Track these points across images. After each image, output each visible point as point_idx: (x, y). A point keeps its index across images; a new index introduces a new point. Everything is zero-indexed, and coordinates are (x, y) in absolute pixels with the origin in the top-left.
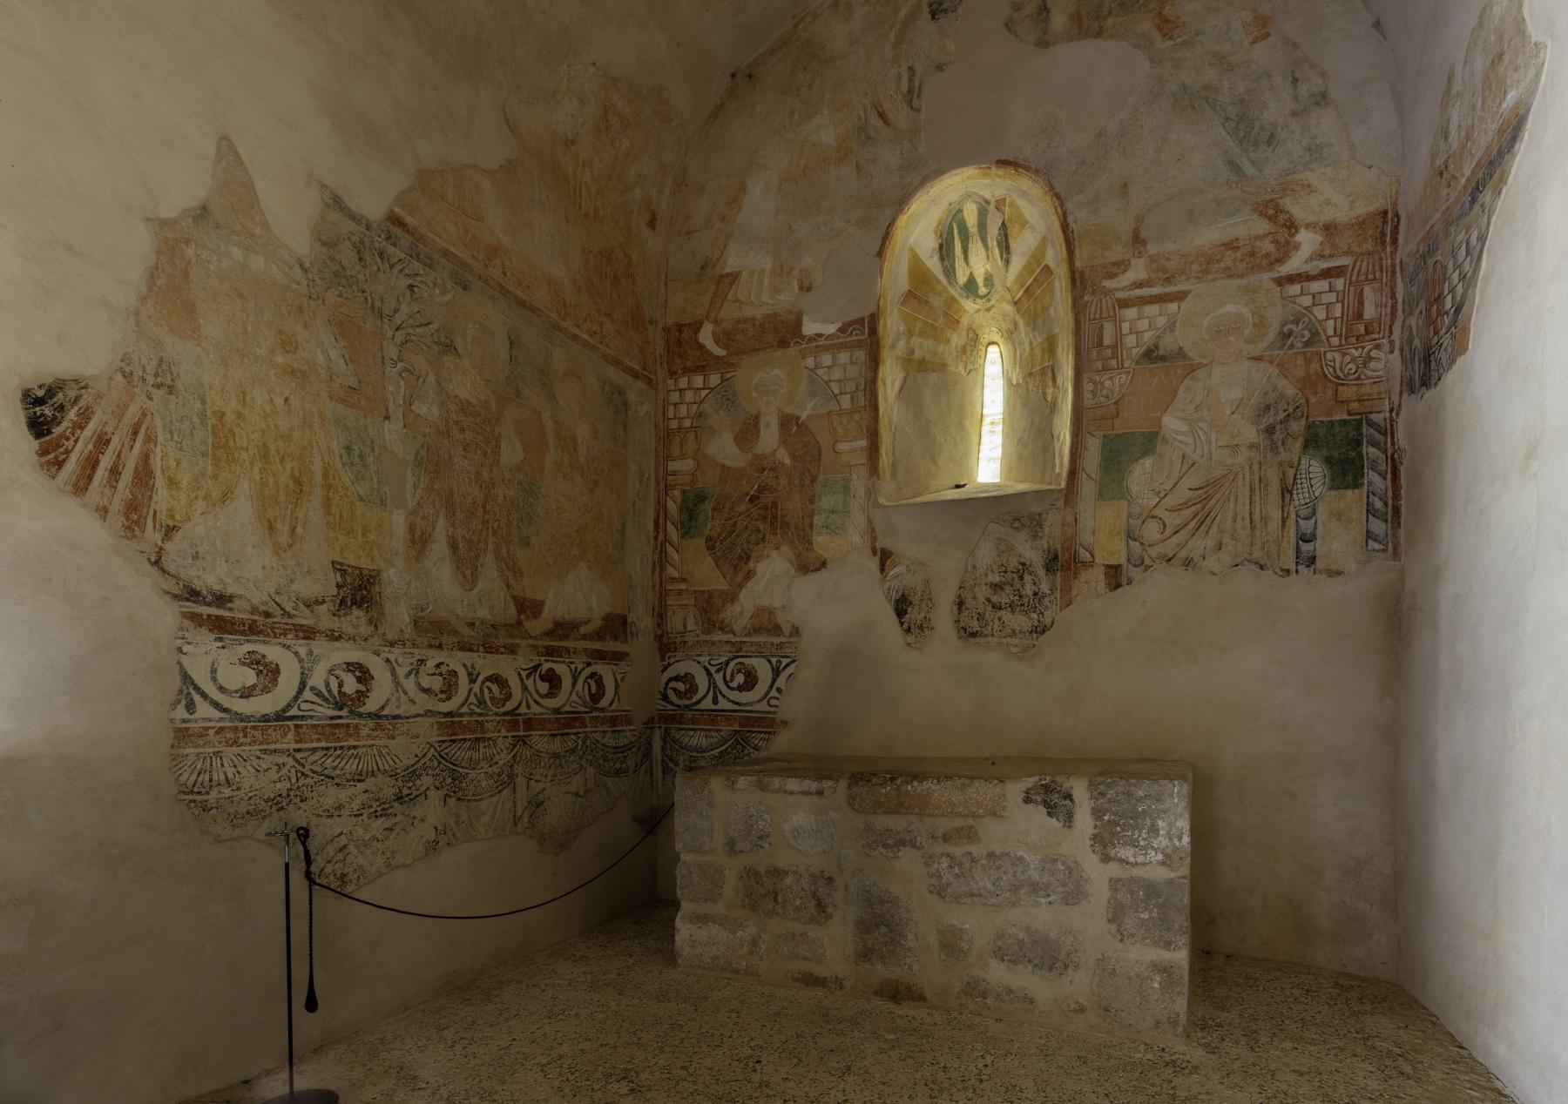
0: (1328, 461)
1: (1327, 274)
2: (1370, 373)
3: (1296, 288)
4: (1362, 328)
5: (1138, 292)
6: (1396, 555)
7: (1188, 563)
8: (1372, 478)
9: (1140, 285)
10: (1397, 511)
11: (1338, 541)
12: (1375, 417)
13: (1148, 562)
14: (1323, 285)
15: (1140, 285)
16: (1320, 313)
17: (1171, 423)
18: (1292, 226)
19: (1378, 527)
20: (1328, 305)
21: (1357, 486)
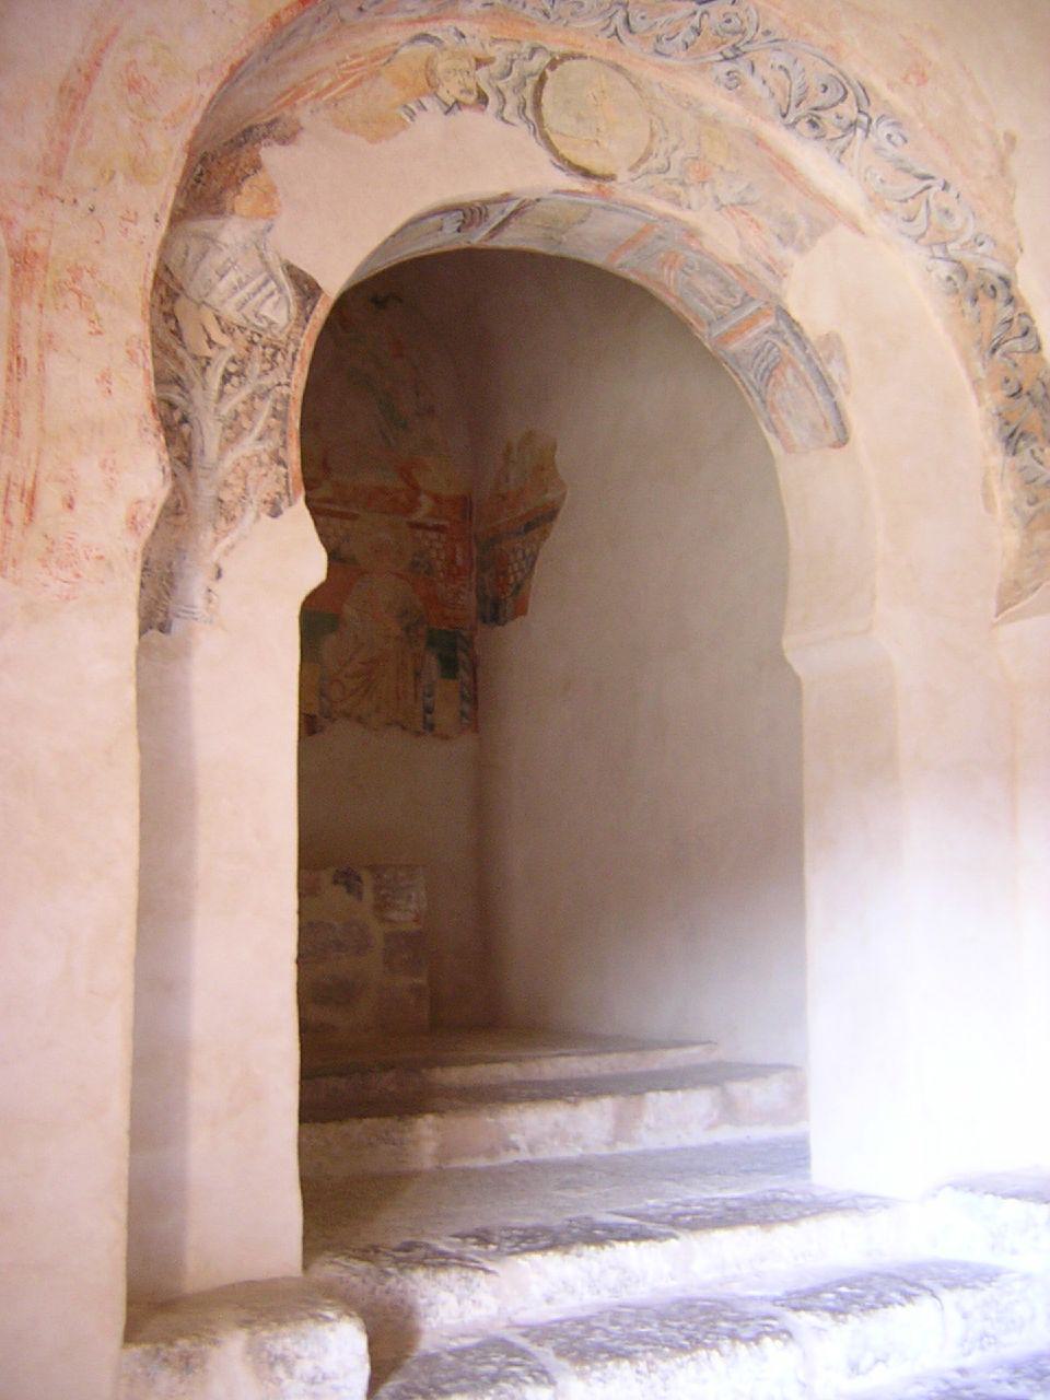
0: (440, 657)
1: (437, 528)
2: (459, 602)
3: (419, 533)
4: (455, 571)
5: (327, 506)
6: (476, 730)
7: (359, 719)
8: (462, 672)
9: (329, 501)
10: (475, 698)
11: (445, 716)
12: (465, 634)
13: (335, 716)
14: (433, 535)
15: (329, 501)
16: (434, 554)
17: (349, 611)
18: (416, 489)
19: (467, 708)
20: (438, 550)
21: (455, 678)
